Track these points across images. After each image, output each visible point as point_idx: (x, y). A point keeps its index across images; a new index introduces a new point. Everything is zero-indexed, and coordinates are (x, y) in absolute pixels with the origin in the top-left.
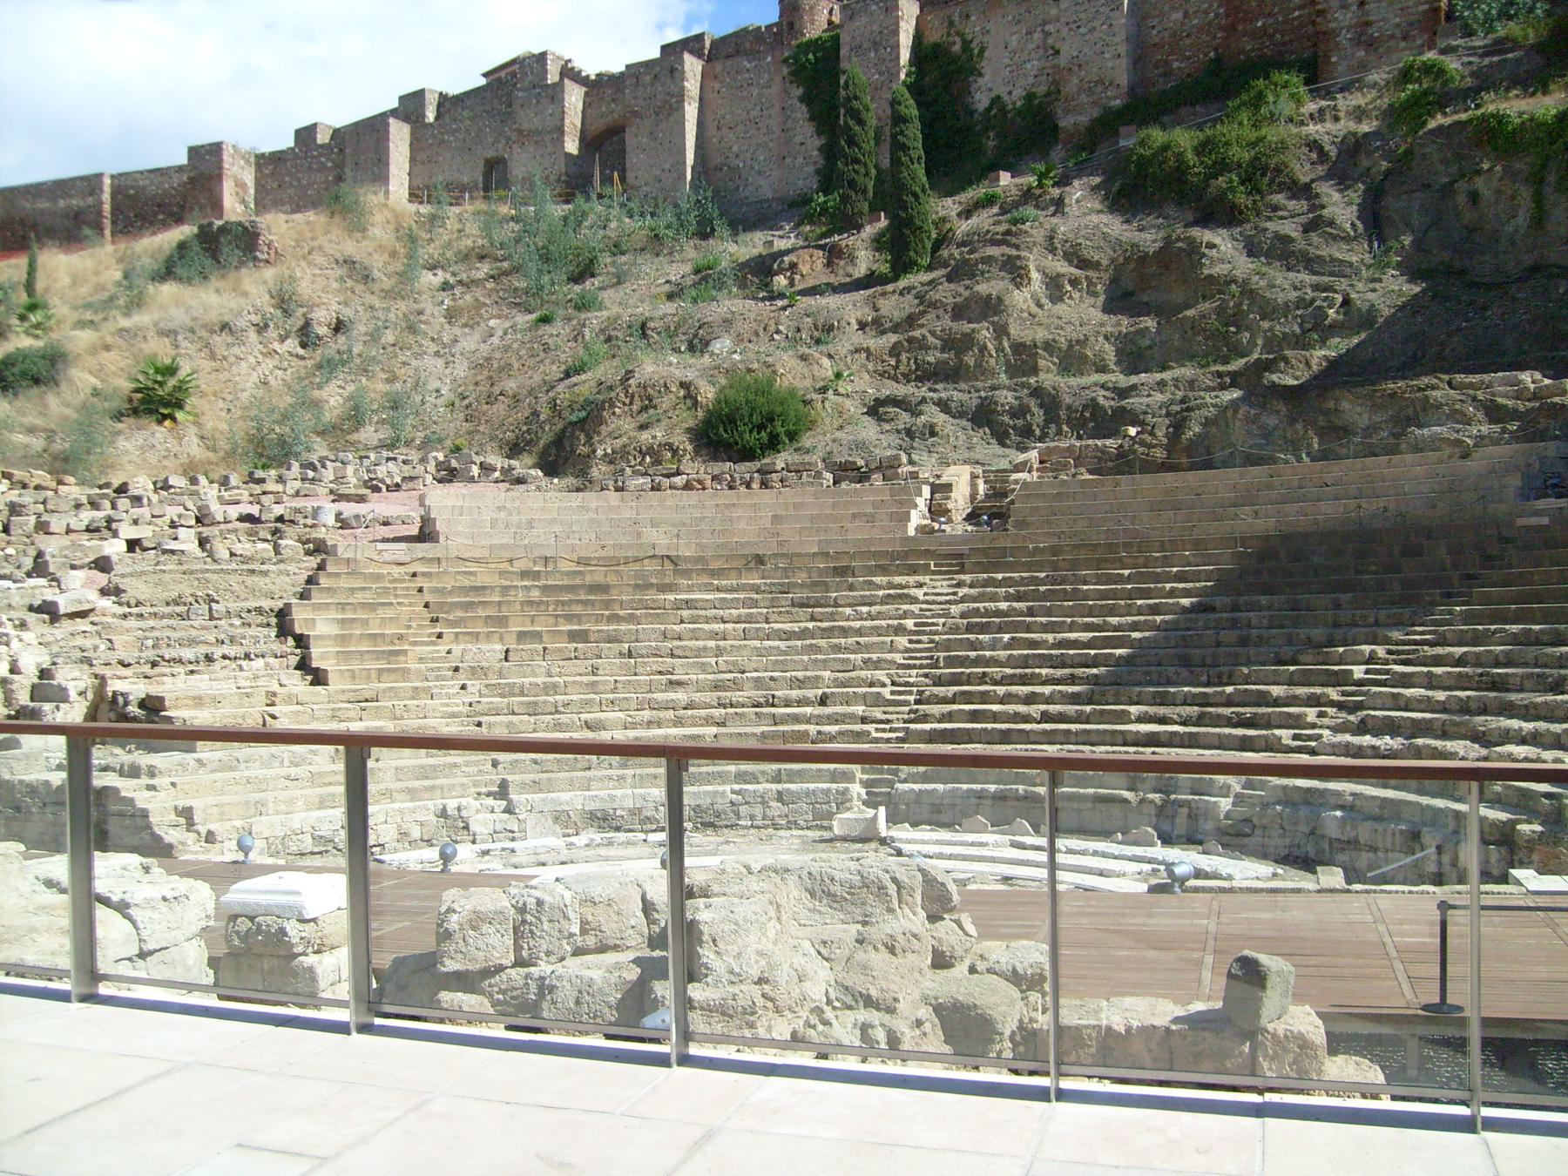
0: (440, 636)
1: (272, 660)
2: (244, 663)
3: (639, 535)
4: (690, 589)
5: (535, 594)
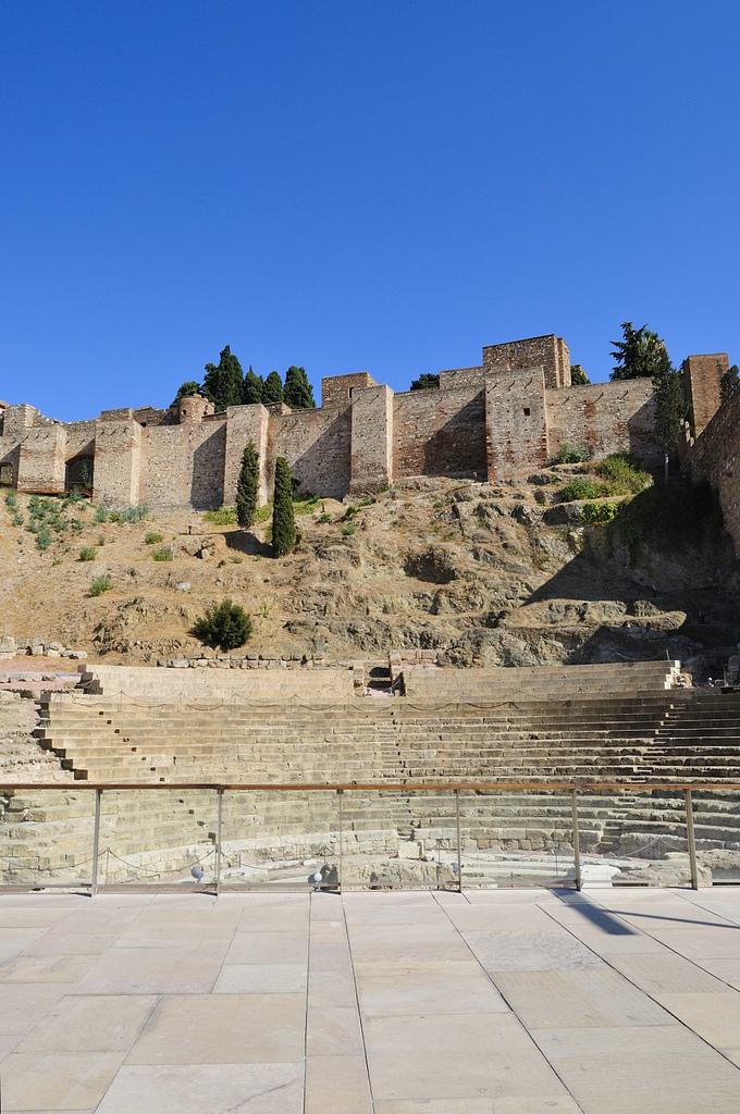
0: (134, 749)
1: (44, 764)
2: (29, 765)
3: (211, 693)
4: (253, 723)
5: (171, 725)
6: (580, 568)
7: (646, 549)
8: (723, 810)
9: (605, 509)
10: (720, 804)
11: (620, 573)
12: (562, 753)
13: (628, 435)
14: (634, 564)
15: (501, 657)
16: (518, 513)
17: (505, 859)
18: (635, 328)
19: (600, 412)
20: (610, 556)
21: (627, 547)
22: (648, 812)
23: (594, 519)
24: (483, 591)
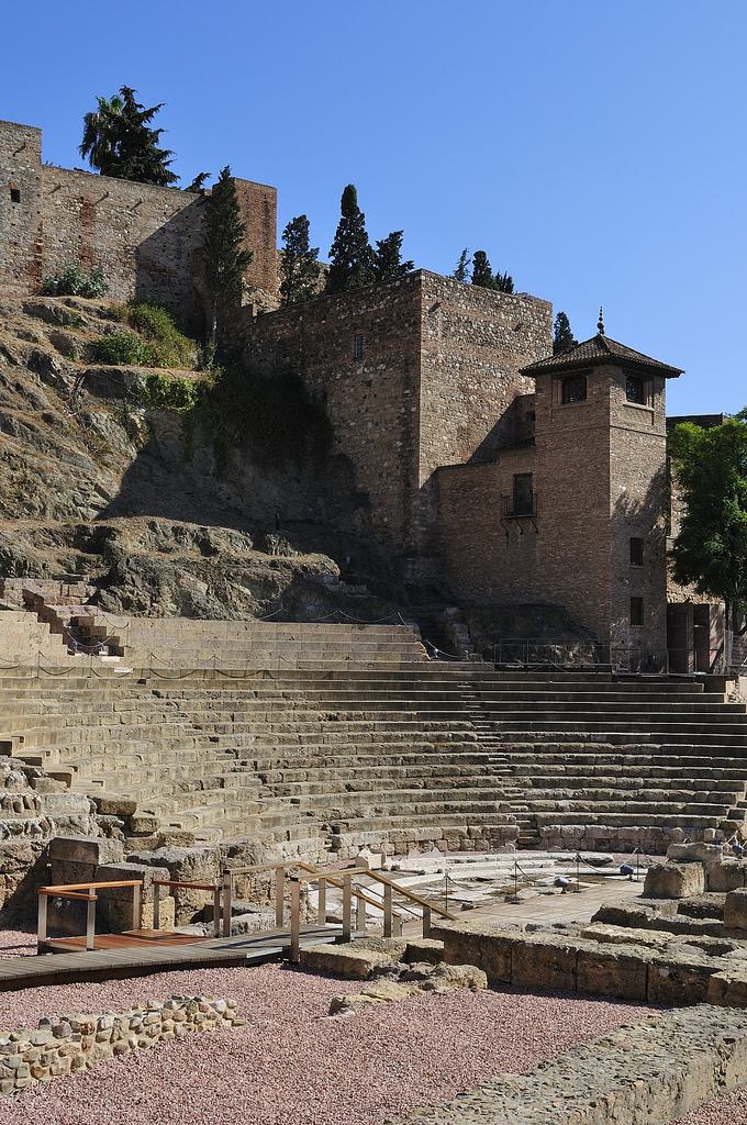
6: (151, 469)
7: (237, 456)
8: (627, 798)
9: (178, 388)
10: (623, 793)
11: (200, 484)
12: (387, 739)
13: (135, 266)
14: (220, 474)
15: (176, 602)
16: (39, 364)
17: (458, 862)
18: (144, 100)
19: (102, 221)
20: (187, 458)
21: (210, 450)
22: (552, 803)
23: (162, 400)
24: (42, 488)
